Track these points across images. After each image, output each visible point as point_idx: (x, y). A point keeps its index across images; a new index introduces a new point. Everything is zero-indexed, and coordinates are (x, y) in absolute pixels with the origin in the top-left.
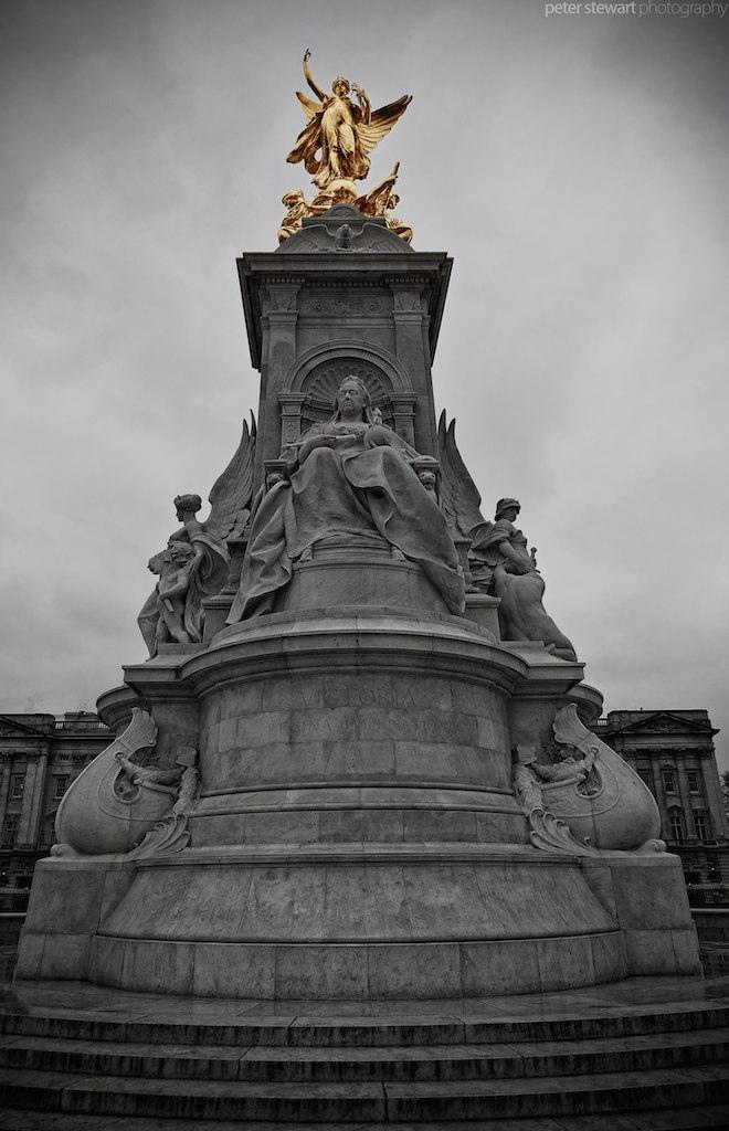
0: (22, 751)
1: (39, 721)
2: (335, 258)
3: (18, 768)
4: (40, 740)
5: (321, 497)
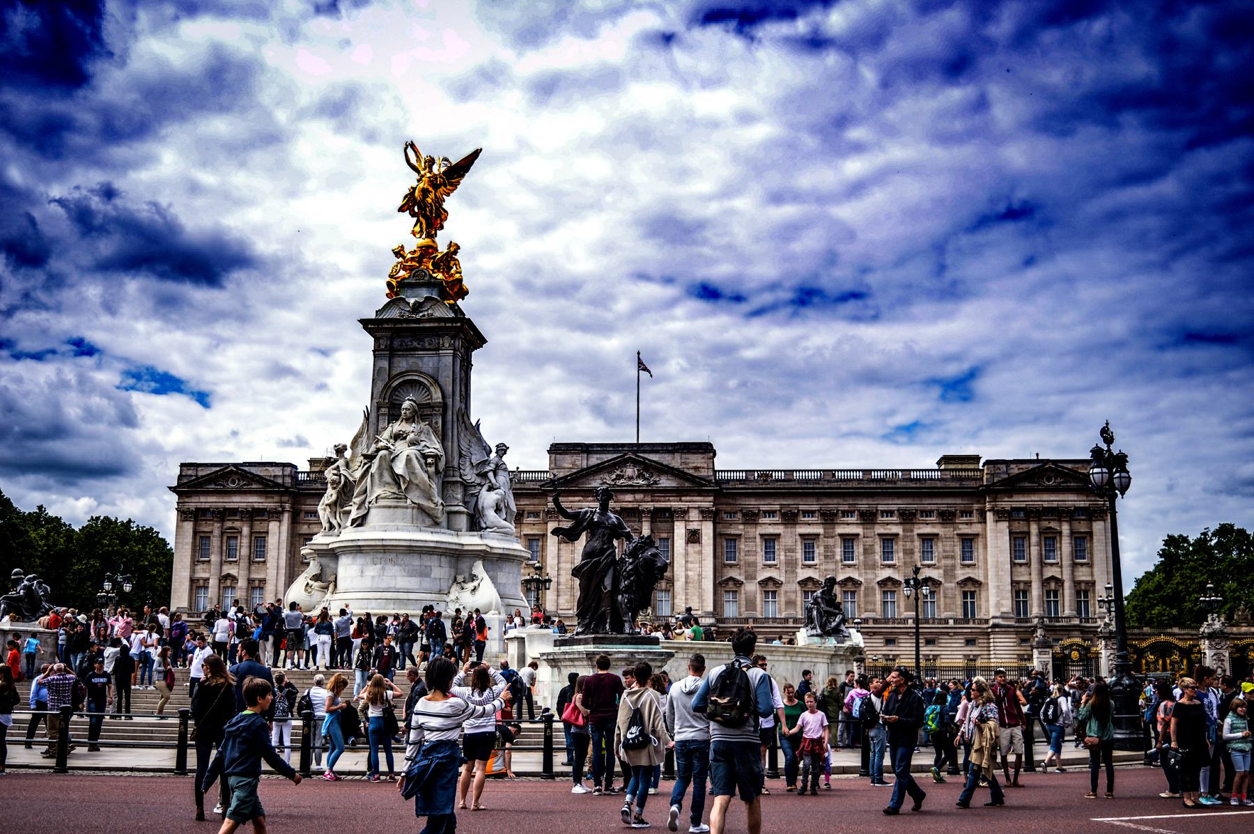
0: (261, 506)
1: (278, 471)
2: (407, 321)
3: (259, 527)
4: (281, 494)
5: (381, 475)
